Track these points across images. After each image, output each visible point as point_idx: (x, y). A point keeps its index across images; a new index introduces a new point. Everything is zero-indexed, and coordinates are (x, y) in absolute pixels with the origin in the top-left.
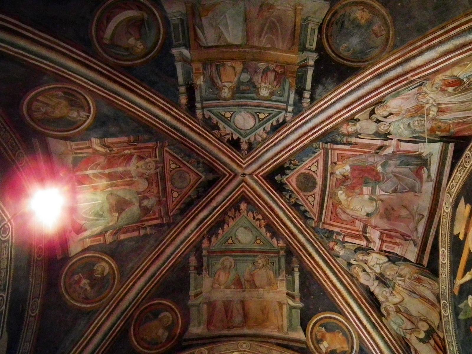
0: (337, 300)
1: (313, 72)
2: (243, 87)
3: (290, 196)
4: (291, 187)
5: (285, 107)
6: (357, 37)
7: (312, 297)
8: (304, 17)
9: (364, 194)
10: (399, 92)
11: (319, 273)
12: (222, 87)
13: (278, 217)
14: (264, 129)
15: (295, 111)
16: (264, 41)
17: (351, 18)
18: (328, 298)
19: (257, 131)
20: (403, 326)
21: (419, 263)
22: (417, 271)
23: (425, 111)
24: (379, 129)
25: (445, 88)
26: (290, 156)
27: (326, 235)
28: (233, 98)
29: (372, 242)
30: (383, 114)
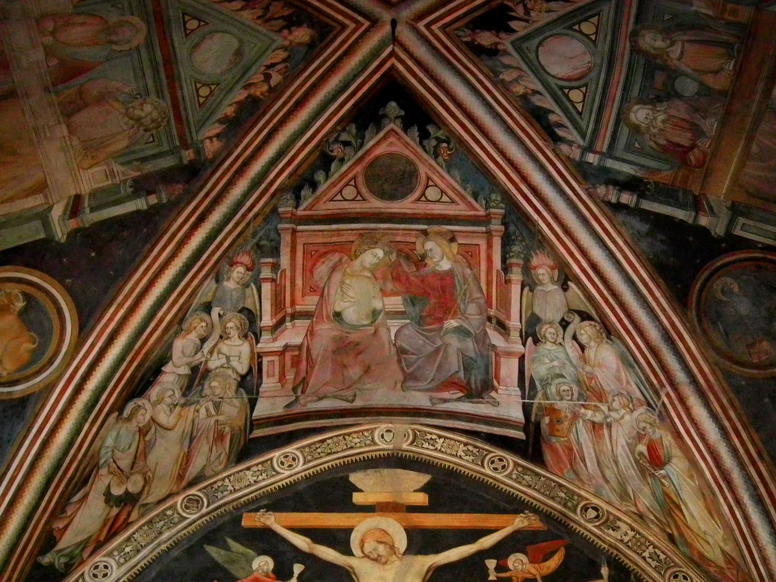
0: (111, 310)
1: (681, 221)
2: (660, 78)
3: (346, 144)
4: (372, 143)
5: (598, 149)
7: (93, 254)
9: (385, 299)
10: (633, 367)
11: (161, 251)
12: (671, 39)
13: (282, 122)
14: (536, 92)
16: (767, 142)
18: (106, 290)
19: (532, 76)
20: (118, 454)
21: (254, 424)
22: (237, 428)
23: (593, 403)
25: (645, 441)
26: (461, 141)
28: (635, 50)
29: (274, 336)
30: (582, 334)
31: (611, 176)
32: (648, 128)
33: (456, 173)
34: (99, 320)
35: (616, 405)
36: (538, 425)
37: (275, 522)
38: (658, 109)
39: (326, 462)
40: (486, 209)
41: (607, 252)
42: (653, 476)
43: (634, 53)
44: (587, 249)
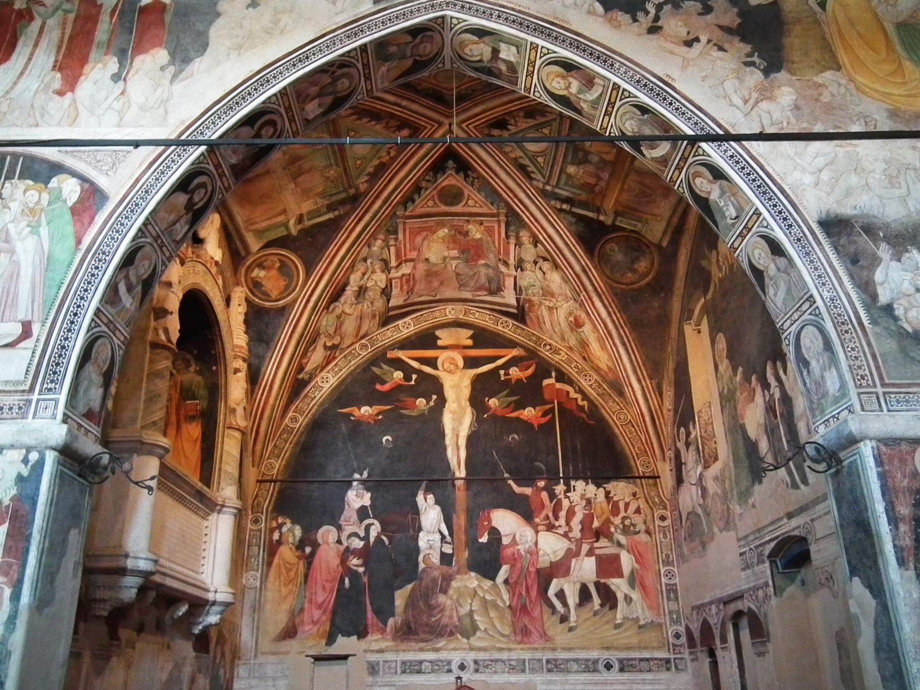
2: (581, 154)
3: (428, 181)
4: (441, 180)
11: (342, 236)
13: (397, 173)
14: (521, 157)
17: (641, 258)
18: (317, 256)
19: (519, 150)
20: (328, 328)
26: (485, 178)
27: (391, 229)
34: (315, 270)
35: (560, 299)
36: (523, 307)
37: (402, 355)
39: (424, 325)
42: (576, 331)
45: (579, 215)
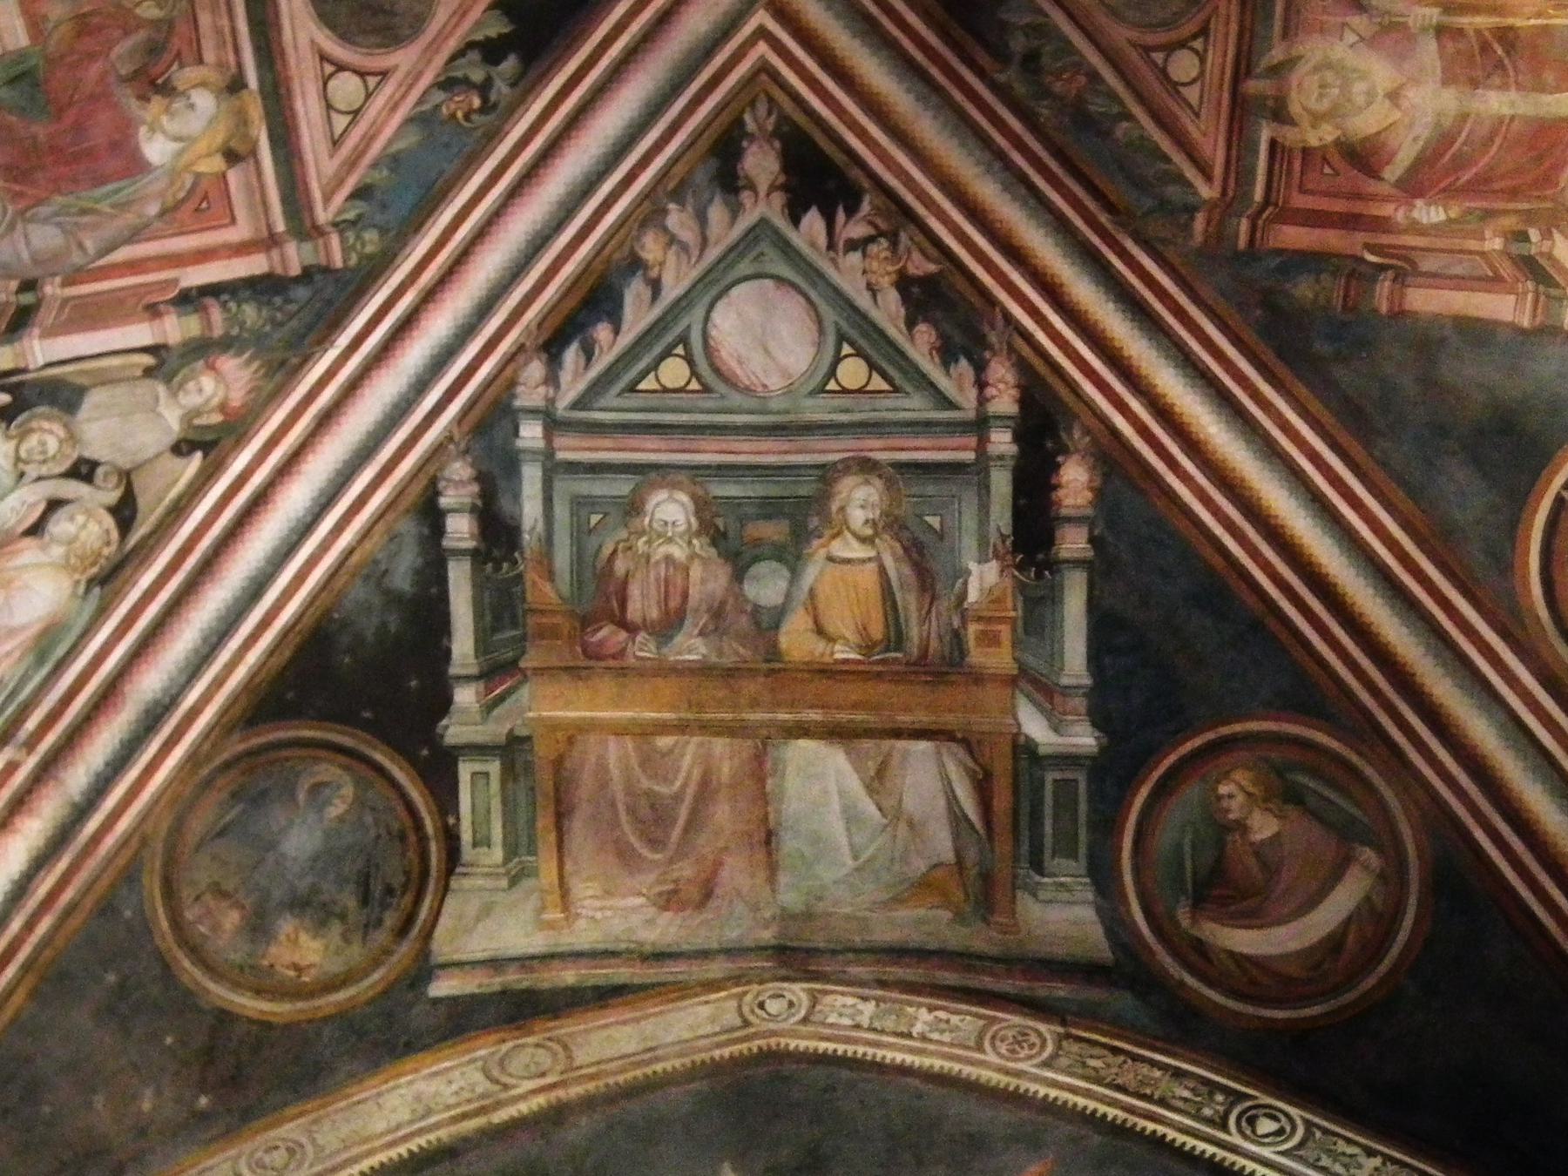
1: (448, 652)
2: (773, 531)
5: (559, 441)
6: (295, 859)
8: (527, 883)
10: (41, 659)
12: (876, 534)
14: (656, 286)
15: (506, 423)
17: (336, 928)
19: (695, 274)
24: (66, 426)
26: (493, 136)
28: (827, 475)
30: (72, 519)
31: (502, 484)
32: (642, 533)
33: (412, 139)
38: (695, 541)
40: (335, 225)
41: (309, 519)
43: (816, 472)
44: (299, 473)
45: (443, 598)
